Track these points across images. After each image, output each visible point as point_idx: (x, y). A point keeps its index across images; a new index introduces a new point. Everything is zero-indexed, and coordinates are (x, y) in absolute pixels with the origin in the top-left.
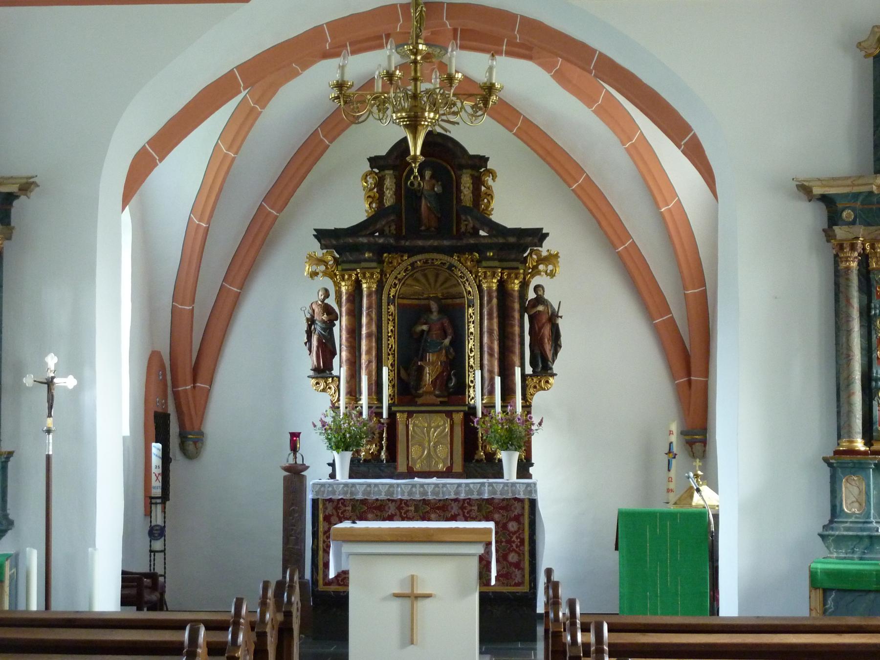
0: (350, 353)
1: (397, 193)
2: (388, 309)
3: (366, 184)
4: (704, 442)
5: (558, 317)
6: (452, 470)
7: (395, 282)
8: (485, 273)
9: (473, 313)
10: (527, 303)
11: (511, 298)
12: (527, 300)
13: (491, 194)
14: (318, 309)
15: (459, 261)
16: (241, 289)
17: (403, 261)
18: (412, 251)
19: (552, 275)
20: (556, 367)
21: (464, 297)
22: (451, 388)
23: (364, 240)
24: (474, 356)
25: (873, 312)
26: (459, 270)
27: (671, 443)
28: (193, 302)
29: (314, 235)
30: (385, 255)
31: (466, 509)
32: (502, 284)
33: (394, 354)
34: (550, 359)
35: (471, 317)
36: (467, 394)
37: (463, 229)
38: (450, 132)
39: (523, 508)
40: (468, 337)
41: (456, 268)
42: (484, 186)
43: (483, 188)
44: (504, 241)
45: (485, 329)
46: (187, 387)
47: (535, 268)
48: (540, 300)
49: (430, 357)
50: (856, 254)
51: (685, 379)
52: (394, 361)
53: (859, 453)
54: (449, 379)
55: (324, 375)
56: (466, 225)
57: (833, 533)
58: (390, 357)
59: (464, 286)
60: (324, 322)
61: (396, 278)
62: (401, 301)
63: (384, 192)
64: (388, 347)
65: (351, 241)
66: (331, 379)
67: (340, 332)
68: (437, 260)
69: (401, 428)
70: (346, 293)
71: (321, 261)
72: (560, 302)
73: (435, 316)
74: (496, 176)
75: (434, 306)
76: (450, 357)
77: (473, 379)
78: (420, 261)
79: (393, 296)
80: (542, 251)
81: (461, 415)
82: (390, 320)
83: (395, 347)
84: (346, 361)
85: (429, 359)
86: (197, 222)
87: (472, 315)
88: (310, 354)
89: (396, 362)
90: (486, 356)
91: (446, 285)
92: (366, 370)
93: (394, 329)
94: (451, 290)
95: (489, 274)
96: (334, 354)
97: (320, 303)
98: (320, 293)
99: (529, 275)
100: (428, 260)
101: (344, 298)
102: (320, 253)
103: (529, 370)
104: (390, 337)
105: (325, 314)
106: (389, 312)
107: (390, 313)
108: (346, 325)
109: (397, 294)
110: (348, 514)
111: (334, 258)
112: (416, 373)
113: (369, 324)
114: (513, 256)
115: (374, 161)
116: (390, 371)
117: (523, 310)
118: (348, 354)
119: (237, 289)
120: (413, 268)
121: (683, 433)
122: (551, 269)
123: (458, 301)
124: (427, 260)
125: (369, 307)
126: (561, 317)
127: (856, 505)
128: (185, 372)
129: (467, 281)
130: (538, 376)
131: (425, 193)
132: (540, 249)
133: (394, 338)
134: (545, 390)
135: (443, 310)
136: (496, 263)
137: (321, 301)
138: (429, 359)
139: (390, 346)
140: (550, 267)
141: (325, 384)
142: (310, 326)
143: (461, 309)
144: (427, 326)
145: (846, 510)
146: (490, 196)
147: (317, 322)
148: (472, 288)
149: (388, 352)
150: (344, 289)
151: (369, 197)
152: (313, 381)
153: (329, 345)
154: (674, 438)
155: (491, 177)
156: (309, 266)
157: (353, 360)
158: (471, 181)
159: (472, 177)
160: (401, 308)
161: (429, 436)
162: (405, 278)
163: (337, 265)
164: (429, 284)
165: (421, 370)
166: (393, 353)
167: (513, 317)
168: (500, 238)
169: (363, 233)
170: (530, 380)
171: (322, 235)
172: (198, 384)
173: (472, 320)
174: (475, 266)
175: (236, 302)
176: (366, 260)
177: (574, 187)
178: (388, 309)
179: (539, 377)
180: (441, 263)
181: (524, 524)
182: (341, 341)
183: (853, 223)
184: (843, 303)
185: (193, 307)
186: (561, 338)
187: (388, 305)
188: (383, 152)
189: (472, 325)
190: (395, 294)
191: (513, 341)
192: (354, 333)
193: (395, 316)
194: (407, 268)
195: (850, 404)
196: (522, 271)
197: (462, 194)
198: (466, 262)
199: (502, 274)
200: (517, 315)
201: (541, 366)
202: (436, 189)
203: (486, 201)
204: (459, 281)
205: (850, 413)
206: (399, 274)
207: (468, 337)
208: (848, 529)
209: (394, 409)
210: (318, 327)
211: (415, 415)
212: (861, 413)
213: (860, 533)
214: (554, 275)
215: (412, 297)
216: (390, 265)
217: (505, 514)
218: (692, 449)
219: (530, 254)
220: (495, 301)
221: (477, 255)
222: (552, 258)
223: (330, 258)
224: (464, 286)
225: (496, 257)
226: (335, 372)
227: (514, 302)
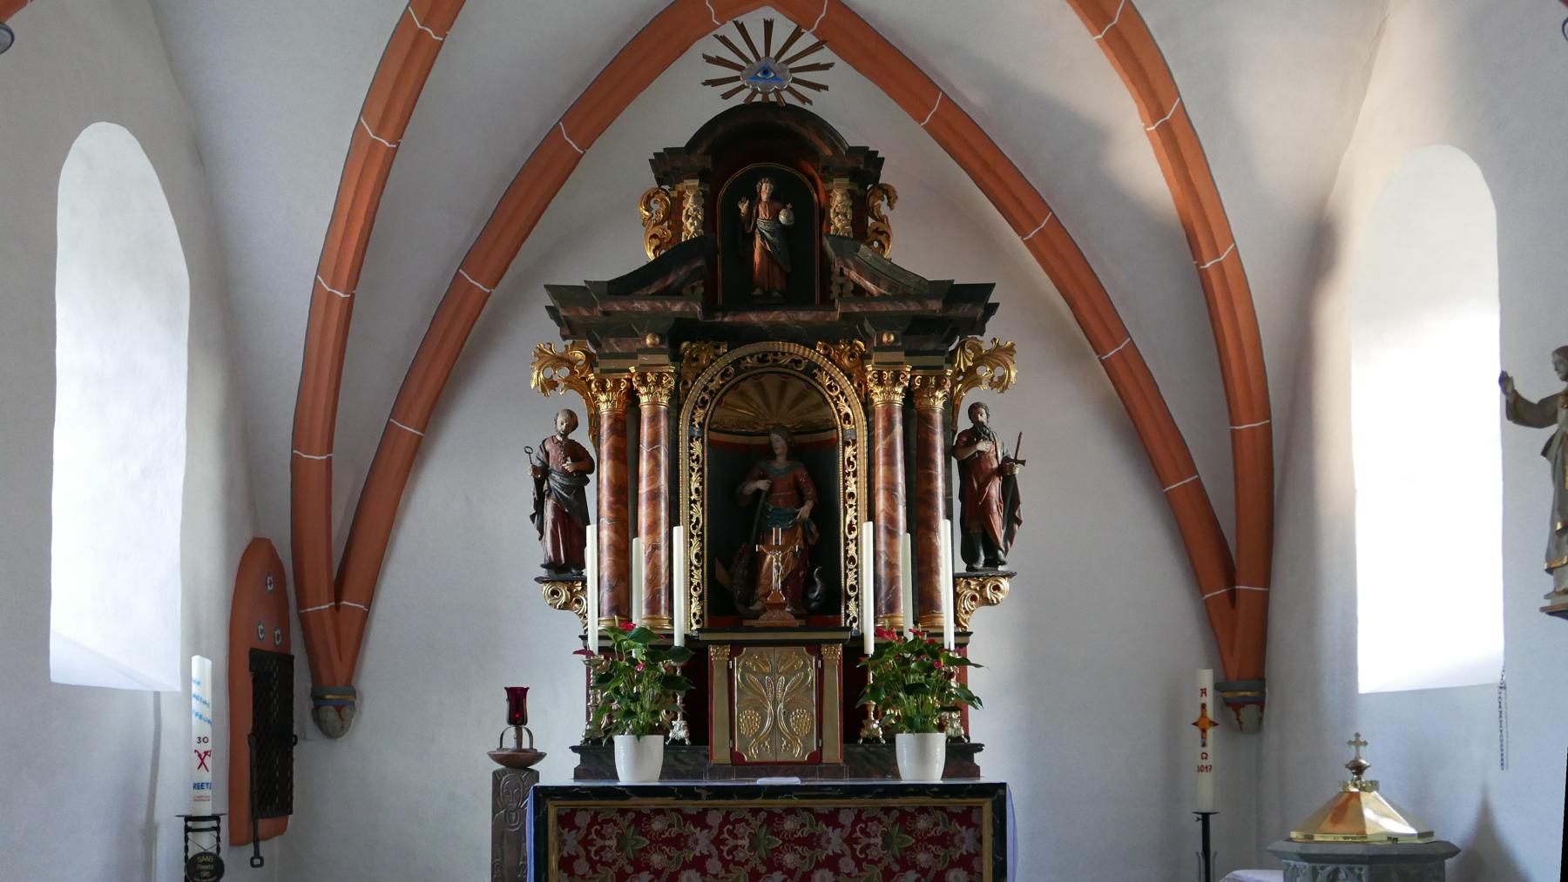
1: (707, 223)
2: (692, 448)
3: (647, 213)
4: (1260, 703)
5: (1017, 462)
6: (821, 759)
7: (704, 398)
8: (880, 374)
9: (855, 457)
10: (956, 439)
11: (930, 427)
12: (955, 432)
13: (886, 229)
14: (556, 451)
15: (827, 356)
16: (423, 431)
18: (739, 337)
19: (1000, 384)
20: (1012, 558)
21: (837, 428)
22: (815, 600)
23: (644, 306)
24: (856, 538)
26: (826, 374)
27: (1203, 706)
28: (330, 449)
29: (548, 308)
30: (684, 345)
31: (858, 844)
33: (702, 536)
35: (850, 463)
36: (843, 612)
38: (810, 102)
39: (980, 840)
40: (845, 502)
41: (820, 369)
42: (874, 217)
43: (871, 221)
44: (920, 308)
46: (322, 607)
47: (971, 371)
48: (978, 432)
49: (777, 535)
51: (1224, 590)
52: (702, 549)
54: (810, 583)
55: (568, 575)
56: (842, 286)
59: (836, 405)
60: (565, 474)
62: (714, 435)
64: (691, 522)
65: (618, 309)
66: (580, 584)
67: (598, 493)
68: (783, 354)
70: (609, 417)
72: (1021, 433)
73: (781, 463)
74: (897, 198)
75: (779, 443)
76: (811, 542)
77: (854, 583)
78: (751, 356)
79: (699, 424)
80: (981, 342)
82: (693, 470)
84: (609, 548)
85: (777, 540)
86: (329, 289)
87: (852, 459)
88: (540, 539)
89: (705, 552)
91: (802, 406)
92: (647, 563)
93: (700, 488)
95: (887, 375)
97: (559, 438)
98: (560, 419)
99: (960, 385)
100: (767, 356)
102: (559, 346)
103: (962, 567)
104: (695, 502)
105: (569, 458)
106: (693, 455)
107: (694, 458)
108: (609, 481)
109: (707, 421)
110: (609, 855)
112: (746, 572)
113: (654, 473)
114: (931, 346)
115: (668, 166)
116: (693, 568)
117: (949, 452)
118: (612, 535)
119: (415, 429)
120: (738, 372)
121: (1218, 687)
122: (1001, 375)
124: (765, 355)
126: (1023, 462)
128: (319, 581)
129: (843, 396)
130: (978, 577)
132: (978, 337)
133: (702, 505)
134: (993, 604)
135: (795, 452)
136: (899, 356)
137: (561, 435)
138: (777, 540)
139: (694, 520)
140: (999, 371)
141: (568, 593)
142: (539, 484)
144: (765, 481)
146: (885, 235)
147: (553, 475)
148: (850, 407)
149: (690, 531)
151: (655, 236)
152: (546, 588)
154: (1209, 700)
155: (886, 200)
156: (539, 369)
160: (712, 446)
162: (723, 391)
163: (592, 367)
164: (768, 404)
166: (700, 533)
168: (911, 303)
169: (643, 292)
170: (963, 584)
172: (345, 603)
173: (850, 470)
174: (857, 366)
176: (646, 351)
177: (1031, 236)
178: (692, 448)
179: (981, 580)
180: (792, 361)
181: (981, 874)
182: (598, 511)
187: (691, 441)
189: (851, 480)
190: (704, 420)
192: (624, 494)
193: (703, 463)
194: (727, 370)
196: (949, 372)
197: (832, 227)
198: (840, 359)
199: (913, 377)
201: (983, 557)
202: (782, 218)
204: (827, 396)
206: (712, 381)
207: (845, 502)
209: (703, 637)
210: (555, 481)
211: (745, 649)
214: (1006, 387)
215: (734, 430)
216: (694, 365)
217: (942, 854)
218: (1238, 714)
219: (962, 345)
220: (898, 429)
221: (862, 345)
222: (1001, 354)
223: (579, 355)
224: (836, 405)
227: (934, 433)
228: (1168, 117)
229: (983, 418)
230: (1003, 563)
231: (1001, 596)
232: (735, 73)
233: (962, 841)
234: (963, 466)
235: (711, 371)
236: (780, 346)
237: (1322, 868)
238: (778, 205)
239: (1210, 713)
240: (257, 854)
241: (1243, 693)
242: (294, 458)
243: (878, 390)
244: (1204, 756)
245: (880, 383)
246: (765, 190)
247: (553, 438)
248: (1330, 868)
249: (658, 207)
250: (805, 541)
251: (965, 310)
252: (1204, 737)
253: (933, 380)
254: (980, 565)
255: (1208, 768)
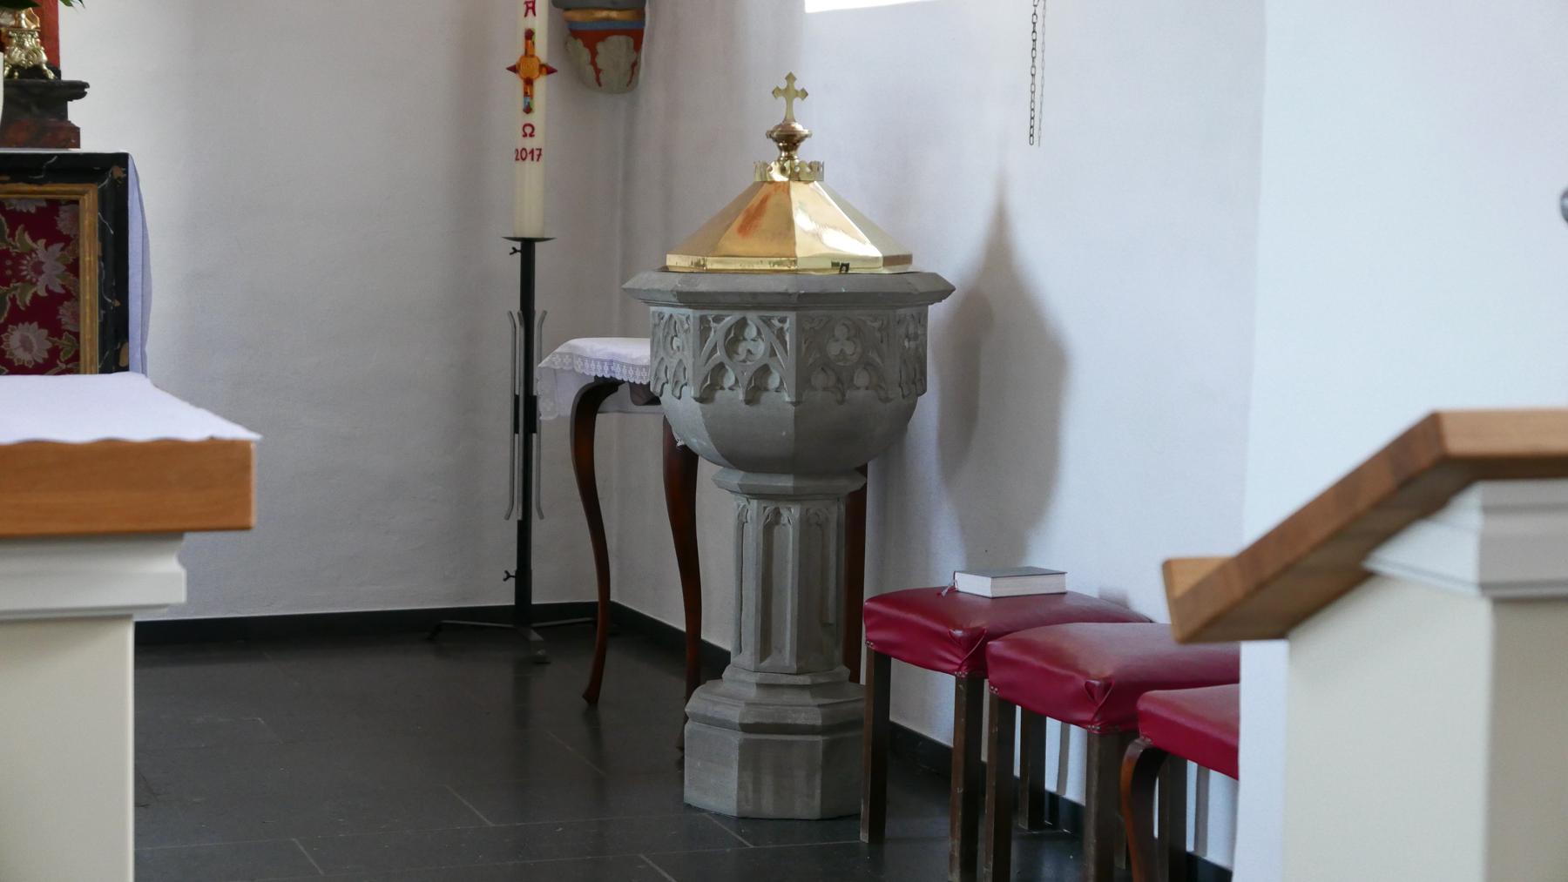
4: (636, 35)
27: (529, 35)
39: (74, 268)
181: (77, 335)
218: (594, 54)
233: (38, 268)
237: (718, 319)
239: (541, 50)
241: (604, 14)
244: (529, 131)
248: (730, 319)
252: (528, 94)
255: (535, 154)
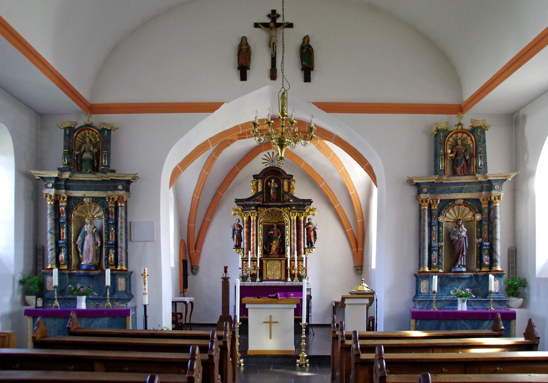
0: (247, 240)
1: (263, 187)
3: (252, 184)
4: (362, 269)
8: (292, 214)
15: (283, 210)
17: (264, 210)
18: (268, 207)
19: (314, 215)
20: (315, 245)
21: (285, 222)
23: (252, 203)
25: (432, 224)
30: (259, 208)
32: (297, 217)
34: (313, 243)
37: (285, 200)
41: (282, 212)
43: (291, 186)
45: (292, 233)
49: (274, 242)
50: (427, 204)
53: (427, 272)
54: (280, 249)
57: (417, 299)
58: (260, 242)
60: (238, 230)
61: (262, 216)
63: (258, 187)
69: (264, 265)
71: (237, 210)
73: (275, 229)
75: (275, 225)
76: (280, 242)
78: (270, 210)
81: (284, 261)
83: (262, 238)
90: (292, 242)
91: (279, 218)
94: (279, 220)
95: (293, 214)
96: (241, 241)
97: (237, 224)
101: (245, 222)
102: (236, 207)
103: (306, 246)
104: (260, 235)
108: (246, 232)
111: (242, 209)
113: (253, 231)
114: (301, 209)
115: (255, 177)
117: (304, 227)
120: (268, 213)
123: (283, 223)
124: (273, 210)
125: (253, 225)
127: (425, 289)
131: (272, 187)
132: (310, 206)
135: (278, 226)
136: (296, 211)
140: (313, 212)
142: (233, 232)
143: (284, 226)
145: (422, 292)
150: (245, 219)
151: (253, 188)
152: (235, 250)
153: (240, 238)
157: (248, 243)
158: (287, 183)
159: (288, 182)
160: (264, 226)
161: (274, 268)
164: (273, 218)
165: (271, 246)
167: (301, 229)
169: (252, 200)
171: (237, 201)
173: (287, 230)
175: (209, 224)
182: (244, 236)
183: (426, 193)
184: (422, 221)
185: (194, 226)
186: (317, 236)
188: (258, 173)
189: (287, 232)
191: (301, 236)
192: (249, 234)
195: (424, 255)
196: (304, 214)
199: (298, 214)
200: (302, 228)
202: (276, 186)
203: (292, 190)
205: (424, 259)
208: (423, 298)
209: (262, 259)
210: (236, 231)
212: (428, 259)
213: (426, 300)
219: (307, 208)
220: (295, 223)
221: (289, 208)
223: (240, 209)
225: (296, 209)
226: (242, 247)
228: (342, 170)
229: (310, 221)
230: (313, 246)
231: (313, 251)
232: (267, 161)
234: (307, 229)
235: (263, 212)
236: (275, 208)
238: (275, 183)
240: (184, 295)
242: (188, 225)
243: (292, 217)
245: (292, 216)
246: (273, 181)
247: (236, 223)
249: (254, 183)
250: (279, 242)
251: (307, 203)
253: (301, 215)
254: (310, 246)
